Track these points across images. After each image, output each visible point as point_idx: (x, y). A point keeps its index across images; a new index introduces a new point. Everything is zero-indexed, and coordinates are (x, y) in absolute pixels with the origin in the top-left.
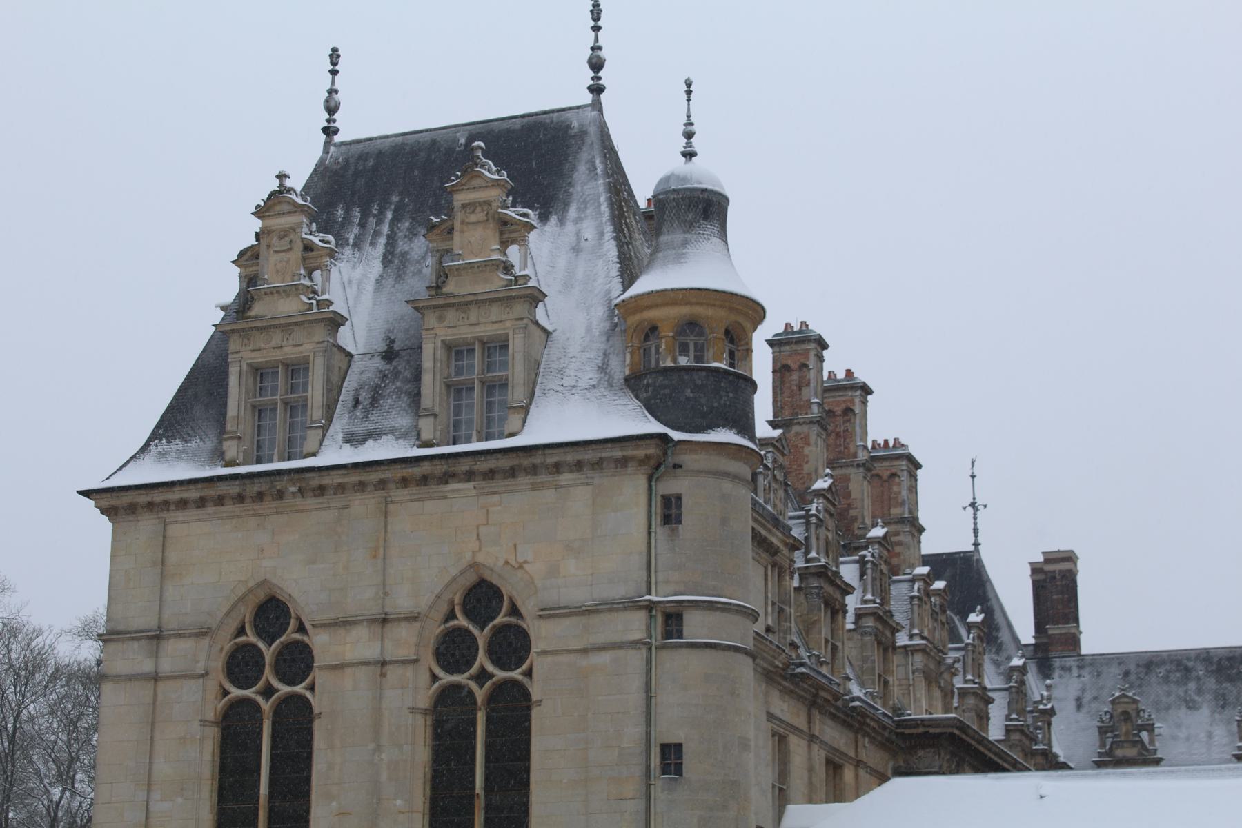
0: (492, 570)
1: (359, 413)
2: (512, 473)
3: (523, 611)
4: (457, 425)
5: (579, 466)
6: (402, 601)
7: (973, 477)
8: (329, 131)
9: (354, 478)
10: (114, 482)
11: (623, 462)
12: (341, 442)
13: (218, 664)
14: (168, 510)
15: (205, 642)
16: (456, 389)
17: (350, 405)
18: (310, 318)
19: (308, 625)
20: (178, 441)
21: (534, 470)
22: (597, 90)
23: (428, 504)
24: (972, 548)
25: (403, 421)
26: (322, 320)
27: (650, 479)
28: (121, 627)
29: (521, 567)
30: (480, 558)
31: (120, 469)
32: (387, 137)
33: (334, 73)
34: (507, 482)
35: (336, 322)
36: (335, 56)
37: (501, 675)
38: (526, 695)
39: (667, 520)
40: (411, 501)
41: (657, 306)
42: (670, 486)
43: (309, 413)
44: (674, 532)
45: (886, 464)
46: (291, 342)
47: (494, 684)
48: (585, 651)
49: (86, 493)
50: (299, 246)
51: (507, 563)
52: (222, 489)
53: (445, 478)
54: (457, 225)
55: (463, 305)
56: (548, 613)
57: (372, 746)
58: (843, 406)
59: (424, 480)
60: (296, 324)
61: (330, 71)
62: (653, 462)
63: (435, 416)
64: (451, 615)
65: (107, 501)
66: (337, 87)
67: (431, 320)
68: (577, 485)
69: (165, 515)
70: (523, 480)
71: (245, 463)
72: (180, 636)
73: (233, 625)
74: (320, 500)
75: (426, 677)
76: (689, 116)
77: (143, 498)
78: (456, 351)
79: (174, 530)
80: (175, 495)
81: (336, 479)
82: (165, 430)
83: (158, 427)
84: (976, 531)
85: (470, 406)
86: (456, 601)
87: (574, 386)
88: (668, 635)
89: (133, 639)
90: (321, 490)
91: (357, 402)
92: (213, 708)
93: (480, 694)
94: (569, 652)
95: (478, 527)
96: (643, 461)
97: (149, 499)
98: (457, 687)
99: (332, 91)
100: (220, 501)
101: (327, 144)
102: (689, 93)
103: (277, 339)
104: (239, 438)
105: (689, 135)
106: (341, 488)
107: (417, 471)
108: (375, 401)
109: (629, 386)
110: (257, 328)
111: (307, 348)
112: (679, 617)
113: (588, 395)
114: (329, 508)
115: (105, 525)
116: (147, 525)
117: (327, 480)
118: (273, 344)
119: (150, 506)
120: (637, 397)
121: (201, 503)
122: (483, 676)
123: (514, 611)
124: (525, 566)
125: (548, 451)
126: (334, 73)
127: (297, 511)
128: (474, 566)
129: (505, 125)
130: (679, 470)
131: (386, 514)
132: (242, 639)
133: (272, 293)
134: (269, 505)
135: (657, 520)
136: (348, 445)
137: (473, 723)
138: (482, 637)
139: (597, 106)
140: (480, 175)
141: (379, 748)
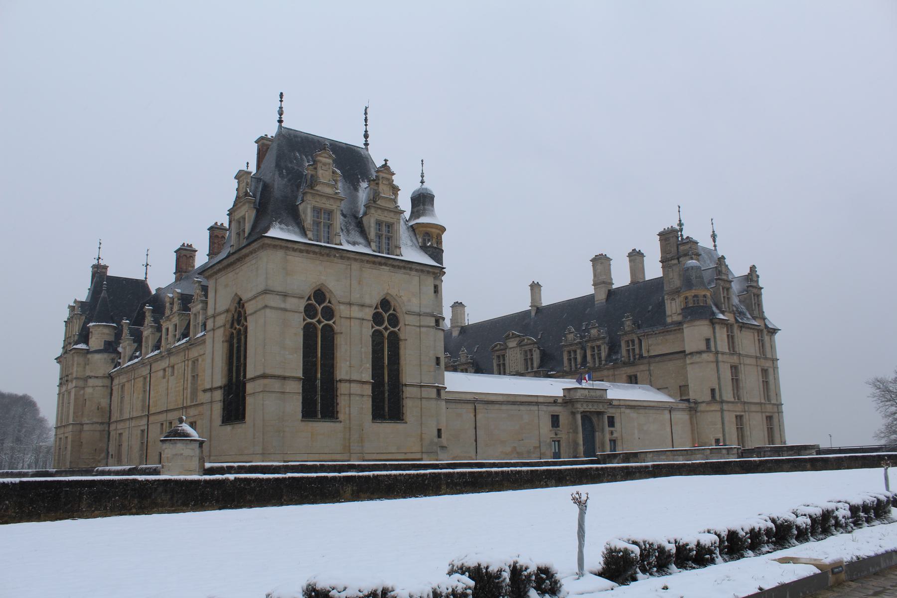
2: (399, 267)
6: (367, 301)
7: (147, 255)
8: (280, 121)
11: (428, 272)
13: (302, 309)
15: (302, 300)
22: (366, 144)
23: (374, 270)
24: (144, 279)
28: (272, 289)
32: (301, 132)
33: (281, 101)
34: (398, 270)
36: (281, 95)
40: (369, 268)
45: (189, 252)
46: (328, 203)
48: (420, 326)
50: (331, 170)
51: (397, 295)
52: (313, 249)
53: (380, 264)
55: (384, 209)
56: (408, 313)
57: (360, 346)
58: (221, 235)
59: (374, 263)
60: (333, 198)
61: (280, 101)
66: (283, 106)
69: (288, 252)
70: (403, 271)
72: (294, 297)
76: (422, 171)
78: (379, 223)
81: (352, 256)
84: (146, 274)
89: (277, 294)
91: (342, 230)
92: (303, 324)
93: (386, 334)
94: (415, 326)
98: (310, 324)
99: (281, 108)
101: (280, 127)
102: (422, 164)
103: (324, 200)
105: (422, 176)
106: (349, 259)
107: (376, 260)
109: (422, 249)
111: (334, 207)
117: (348, 255)
118: (323, 201)
120: (427, 254)
122: (386, 329)
125: (414, 264)
126: (281, 101)
128: (388, 294)
129: (340, 144)
132: (310, 302)
133: (326, 185)
137: (383, 343)
139: (367, 149)
141: (362, 348)
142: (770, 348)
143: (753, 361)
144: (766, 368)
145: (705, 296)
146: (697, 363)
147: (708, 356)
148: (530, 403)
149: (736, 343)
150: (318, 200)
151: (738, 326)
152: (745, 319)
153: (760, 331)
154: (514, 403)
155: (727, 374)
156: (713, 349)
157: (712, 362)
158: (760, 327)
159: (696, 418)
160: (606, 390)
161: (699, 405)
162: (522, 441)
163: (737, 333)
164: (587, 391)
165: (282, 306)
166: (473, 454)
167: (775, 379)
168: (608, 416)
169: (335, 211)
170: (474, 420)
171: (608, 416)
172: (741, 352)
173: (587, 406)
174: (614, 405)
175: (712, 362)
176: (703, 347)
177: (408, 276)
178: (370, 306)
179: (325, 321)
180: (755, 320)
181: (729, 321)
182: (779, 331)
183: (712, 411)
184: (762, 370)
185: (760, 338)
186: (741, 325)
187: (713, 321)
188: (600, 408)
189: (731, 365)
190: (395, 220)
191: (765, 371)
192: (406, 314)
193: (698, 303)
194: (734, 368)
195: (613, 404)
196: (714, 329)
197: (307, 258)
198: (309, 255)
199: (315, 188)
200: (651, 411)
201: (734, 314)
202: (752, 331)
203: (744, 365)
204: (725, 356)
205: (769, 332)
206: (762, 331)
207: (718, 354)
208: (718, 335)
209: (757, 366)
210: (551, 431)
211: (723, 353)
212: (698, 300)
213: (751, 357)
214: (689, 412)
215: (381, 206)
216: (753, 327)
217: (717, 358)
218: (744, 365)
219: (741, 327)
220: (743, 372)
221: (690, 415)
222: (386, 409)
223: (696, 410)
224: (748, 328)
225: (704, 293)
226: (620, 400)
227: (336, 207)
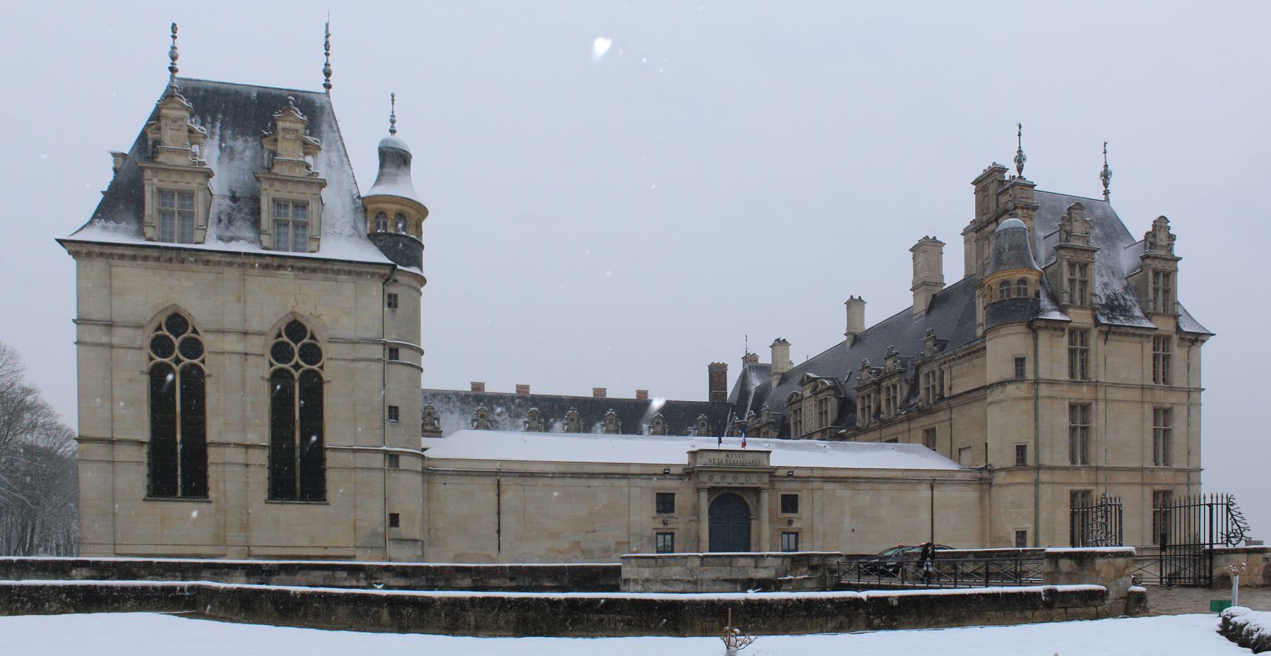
0: (303, 316)
1: (222, 225)
2: (314, 270)
3: (318, 337)
4: (279, 241)
5: (349, 273)
9: (229, 259)
10: (78, 237)
12: (216, 240)
14: (113, 259)
16: (280, 224)
17: (216, 220)
18: (194, 169)
19: (199, 330)
20: (112, 222)
21: (326, 271)
25: (251, 234)
26: (204, 172)
27: (384, 284)
29: (318, 317)
30: (297, 310)
31: (81, 229)
35: (209, 174)
37: (307, 367)
38: (320, 378)
39: (390, 305)
41: (391, 203)
42: (393, 290)
43: (196, 220)
44: (394, 312)
47: (304, 370)
49: (61, 241)
51: (311, 314)
53: (279, 267)
54: (279, 138)
62: (386, 277)
63: (270, 235)
64: (279, 335)
65: (75, 248)
67: (265, 185)
68: (347, 282)
69: (111, 261)
70: (320, 275)
71: (159, 241)
73: (155, 325)
74: (206, 267)
75: (267, 365)
77: (97, 249)
79: (114, 269)
80: (119, 251)
81: (217, 258)
82: (102, 214)
83: (96, 212)
85: (286, 234)
86: (282, 329)
87: (341, 234)
88: (391, 358)
90: (207, 263)
95: (295, 295)
96: (382, 276)
97: (101, 251)
100: (146, 258)
104: (154, 227)
106: (219, 263)
108: (231, 221)
110: (162, 169)
112: (397, 351)
113: (350, 239)
114: (211, 272)
115: (71, 262)
116: (98, 265)
117: (211, 257)
119: (101, 254)
120: (375, 245)
121: (134, 258)
123: (313, 337)
124: (321, 317)
127: (191, 271)
128: (293, 313)
130: (396, 284)
131: (244, 280)
134: (175, 265)
135: (386, 304)
136: (221, 241)
138: (296, 348)
140: (292, 115)
142: (1186, 370)
143: (1136, 395)
144: (1167, 406)
145: (1023, 281)
146: (997, 402)
147: (1017, 388)
148: (608, 476)
149: (1092, 363)
150: (164, 178)
151: (1100, 331)
152: (1122, 318)
153: (1161, 341)
154: (575, 475)
155: (1064, 421)
156: (1029, 375)
157: (1025, 399)
158: (1157, 332)
159: (990, 495)
160: (769, 452)
161: (996, 474)
162: (594, 534)
163: (1096, 345)
164: (724, 455)
165: (104, 339)
166: (493, 551)
167: (1189, 425)
168: (782, 495)
169: (196, 192)
170: (497, 501)
171: (782, 495)
172: (1101, 379)
173: (723, 478)
174: (796, 477)
175: (1025, 399)
176: (1009, 371)
177: (334, 283)
178: (261, 334)
179: (185, 359)
180: (1150, 320)
181: (1071, 324)
182: (1211, 338)
183: (1015, 484)
184: (1156, 411)
185: (1161, 351)
186: (1105, 329)
187: (1034, 325)
188: (753, 482)
189: (1070, 403)
190: (309, 196)
191: (1163, 414)
192: (329, 342)
193: (1009, 295)
194: (1080, 411)
195: (794, 475)
196: (1036, 339)
197: (146, 268)
198: (148, 263)
199: (158, 160)
200: (886, 486)
201: (1094, 310)
202: (1137, 339)
203: (1106, 401)
204: (1058, 388)
205: (1182, 339)
206: (1167, 339)
207: (1038, 383)
208: (1041, 350)
209: (1143, 402)
210: (654, 518)
211: (1051, 383)
212: (1008, 290)
213: (1127, 387)
214: (979, 487)
215: (281, 175)
216: (1138, 332)
217: (1037, 391)
218: (1106, 401)
219: (1107, 333)
220: (1101, 415)
221: (981, 491)
222: (298, 485)
223: (990, 484)
224: (1127, 334)
225: (1020, 276)
226: (812, 468)
227: (196, 185)
